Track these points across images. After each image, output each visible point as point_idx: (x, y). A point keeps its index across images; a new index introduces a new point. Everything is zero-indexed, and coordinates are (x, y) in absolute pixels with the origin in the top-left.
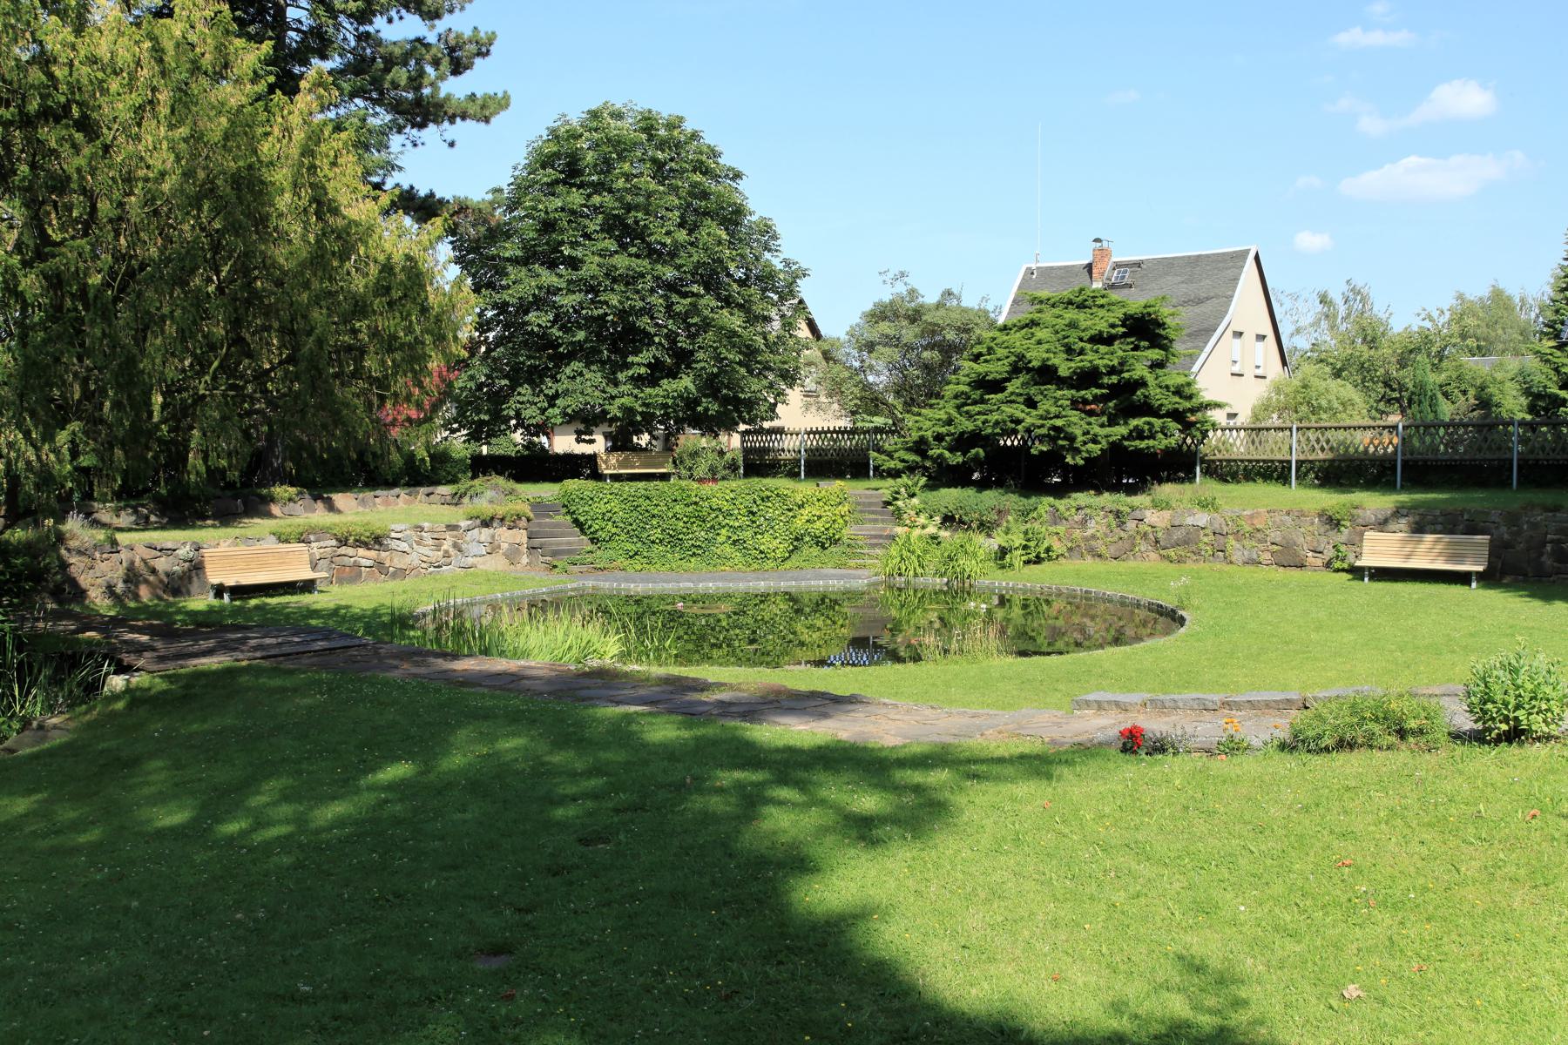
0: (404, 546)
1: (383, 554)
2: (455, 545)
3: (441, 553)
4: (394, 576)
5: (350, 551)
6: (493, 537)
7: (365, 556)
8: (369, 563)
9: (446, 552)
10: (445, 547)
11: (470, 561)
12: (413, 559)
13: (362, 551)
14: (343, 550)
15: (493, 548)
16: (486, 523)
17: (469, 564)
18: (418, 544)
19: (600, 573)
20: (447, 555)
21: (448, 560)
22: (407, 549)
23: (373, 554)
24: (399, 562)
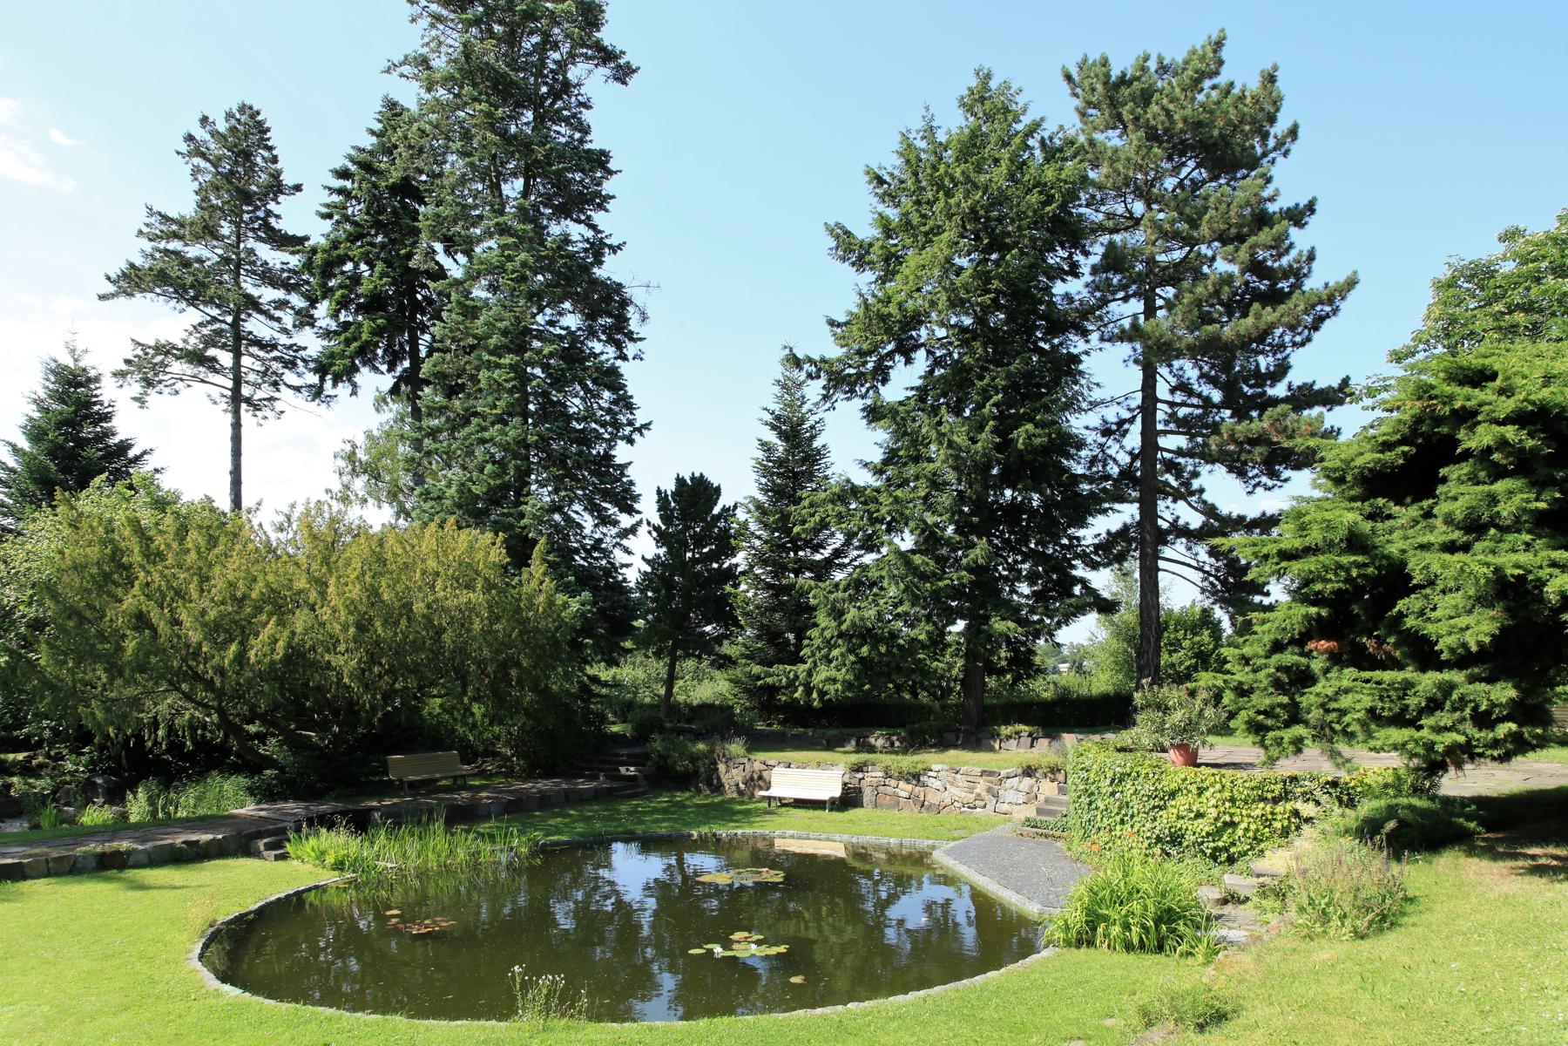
1: (917, 789)
2: (989, 790)
3: (973, 796)
4: (929, 809)
5: (893, 782)
6: (1032, 787)
7: (904, 789)
9: (979, 795)
10: (977, 791)
11: (1005, 807)
13: (902, 784)
15: (1031, 797)
16: (1029, 772)
17: (1004, 810)
18: (952, 785)
19: (1043, 839)
20: (979, 797)
23: (910, 787)
24: (933, 798)
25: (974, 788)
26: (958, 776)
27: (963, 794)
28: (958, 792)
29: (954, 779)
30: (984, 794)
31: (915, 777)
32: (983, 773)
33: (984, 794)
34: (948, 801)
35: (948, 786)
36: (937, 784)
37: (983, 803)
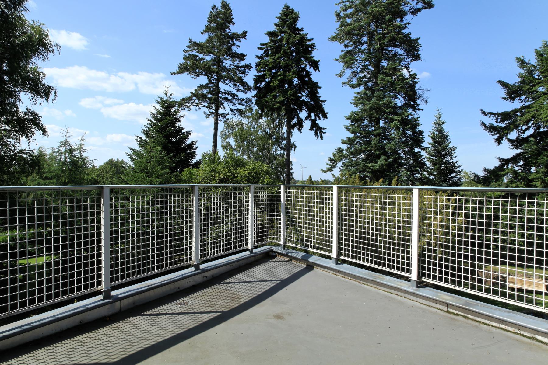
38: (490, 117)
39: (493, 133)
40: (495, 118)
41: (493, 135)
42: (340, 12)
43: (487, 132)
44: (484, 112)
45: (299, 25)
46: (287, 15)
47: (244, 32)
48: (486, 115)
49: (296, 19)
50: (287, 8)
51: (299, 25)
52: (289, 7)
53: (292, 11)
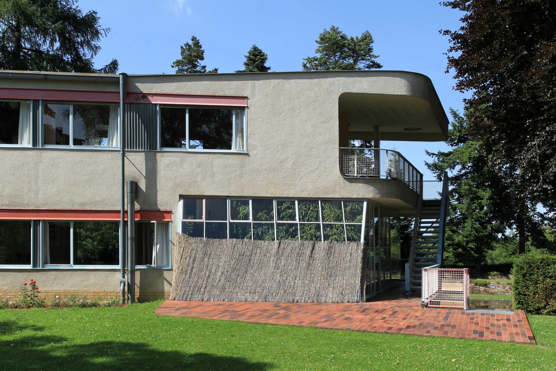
0: (493, 287)
1: (487, 288)
4: (491, 293)
5: (478, 287)
7: (482, 289)
8: (482, 290)
12: (496, 290)
13: (481, 287)
14: (476, 286)
18: (498, 287)
20: (507, 290)
21: (508, 292)
22: (494, 288)
23: (484, 288)
24: (491, 291)
25: (505, 288)
26: (500, 285)
27: (502, 290)
28: (500, 289)
29: (499, 286)
30: (508, 289)
31: (486, 285)
32: (508, 284)
33: (508, 289)
34: (497, 291)
35: (497, 287)
36: (493, 287)
37: (508, 292)
38: (432, 157)
39: (434, 172)
40: (437, 158)
41: (434, 173)
42: (307, 63)
43: (430, 171)
44: (428, 153)
45: (267, 65)
46: (255, 56)
47: (215, 69)
48: (430, 155)
49: (264, 60)
50: (255, 49)
51: (267, 65)
52: (257, 48)
53: (260, 52)
